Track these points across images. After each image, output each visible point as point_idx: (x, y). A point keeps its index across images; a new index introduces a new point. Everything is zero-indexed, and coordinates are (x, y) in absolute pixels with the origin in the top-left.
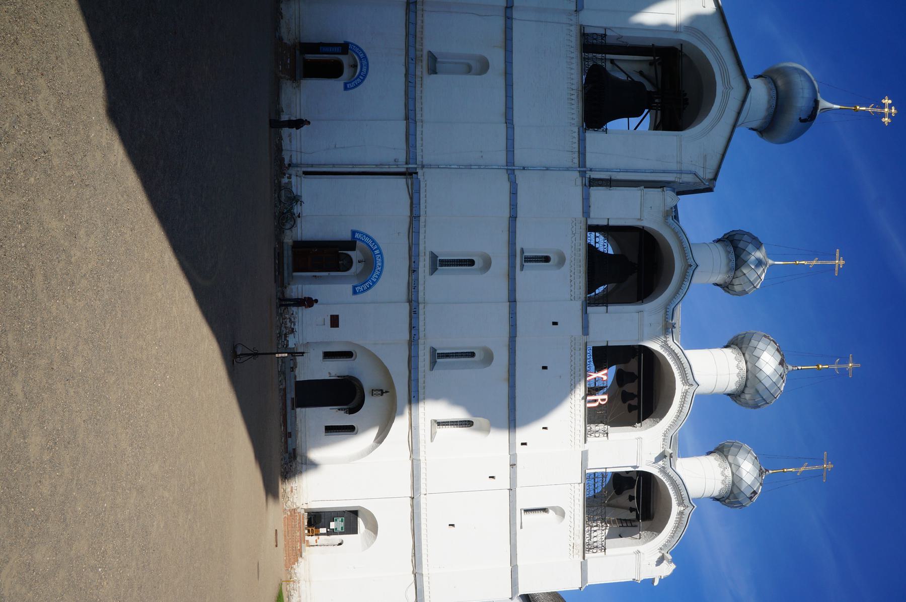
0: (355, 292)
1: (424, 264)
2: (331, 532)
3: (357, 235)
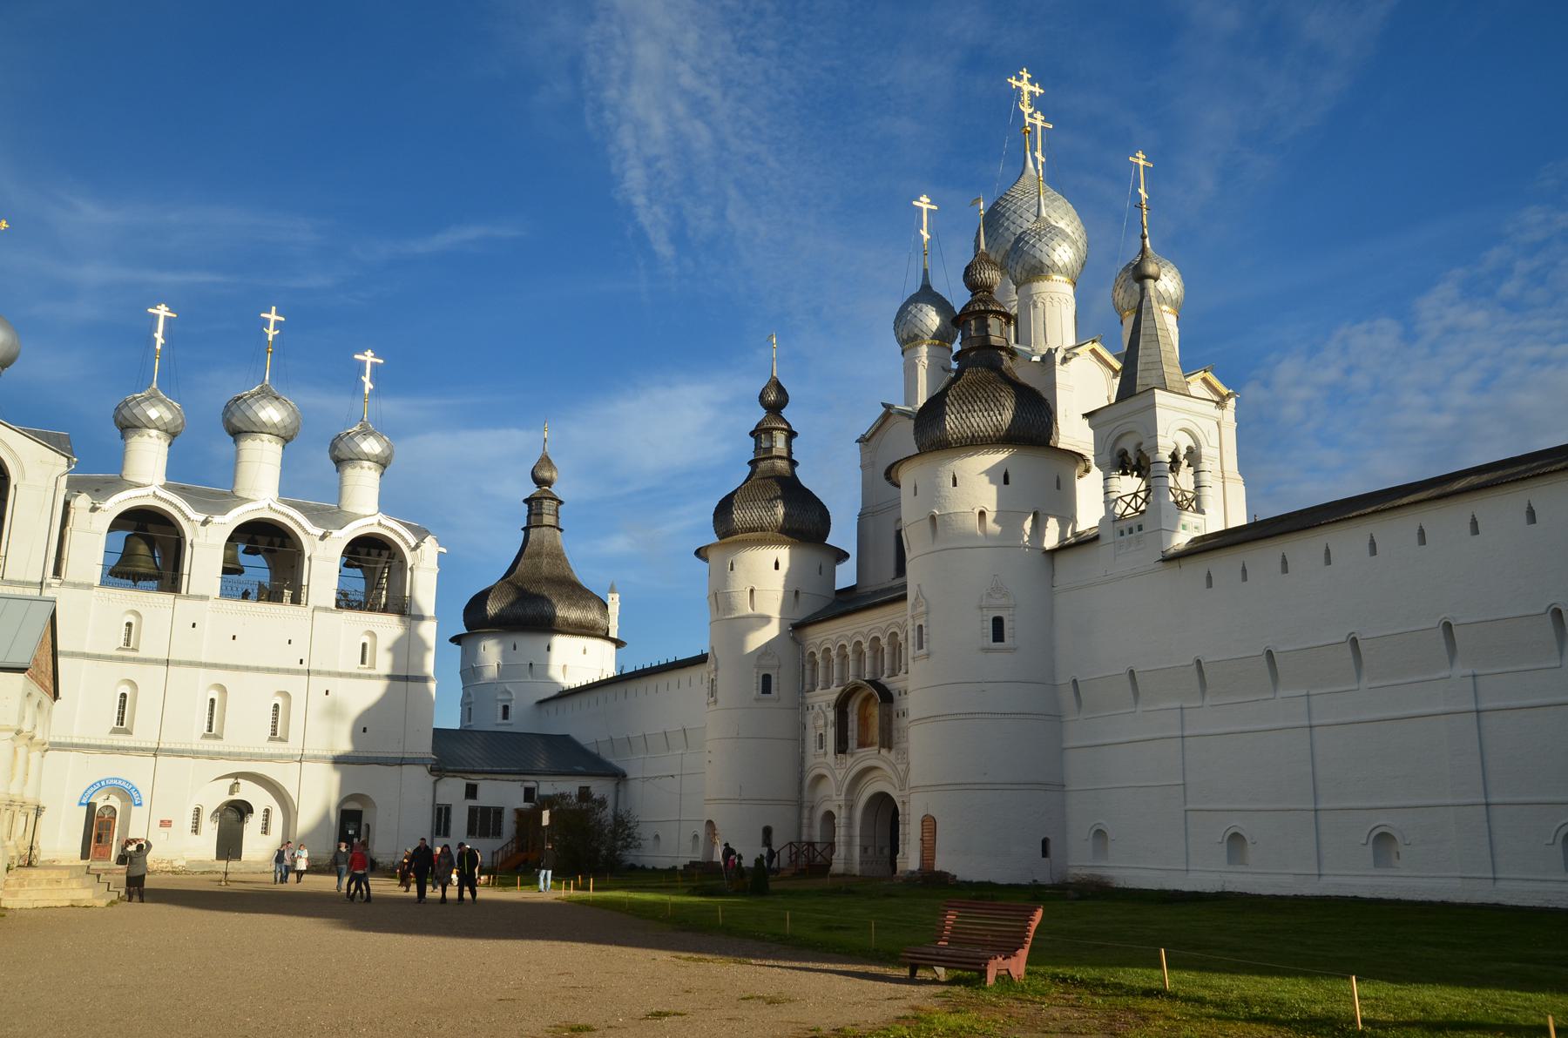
0: (140, 804)
2: (358, 834)
3: (84, 801)
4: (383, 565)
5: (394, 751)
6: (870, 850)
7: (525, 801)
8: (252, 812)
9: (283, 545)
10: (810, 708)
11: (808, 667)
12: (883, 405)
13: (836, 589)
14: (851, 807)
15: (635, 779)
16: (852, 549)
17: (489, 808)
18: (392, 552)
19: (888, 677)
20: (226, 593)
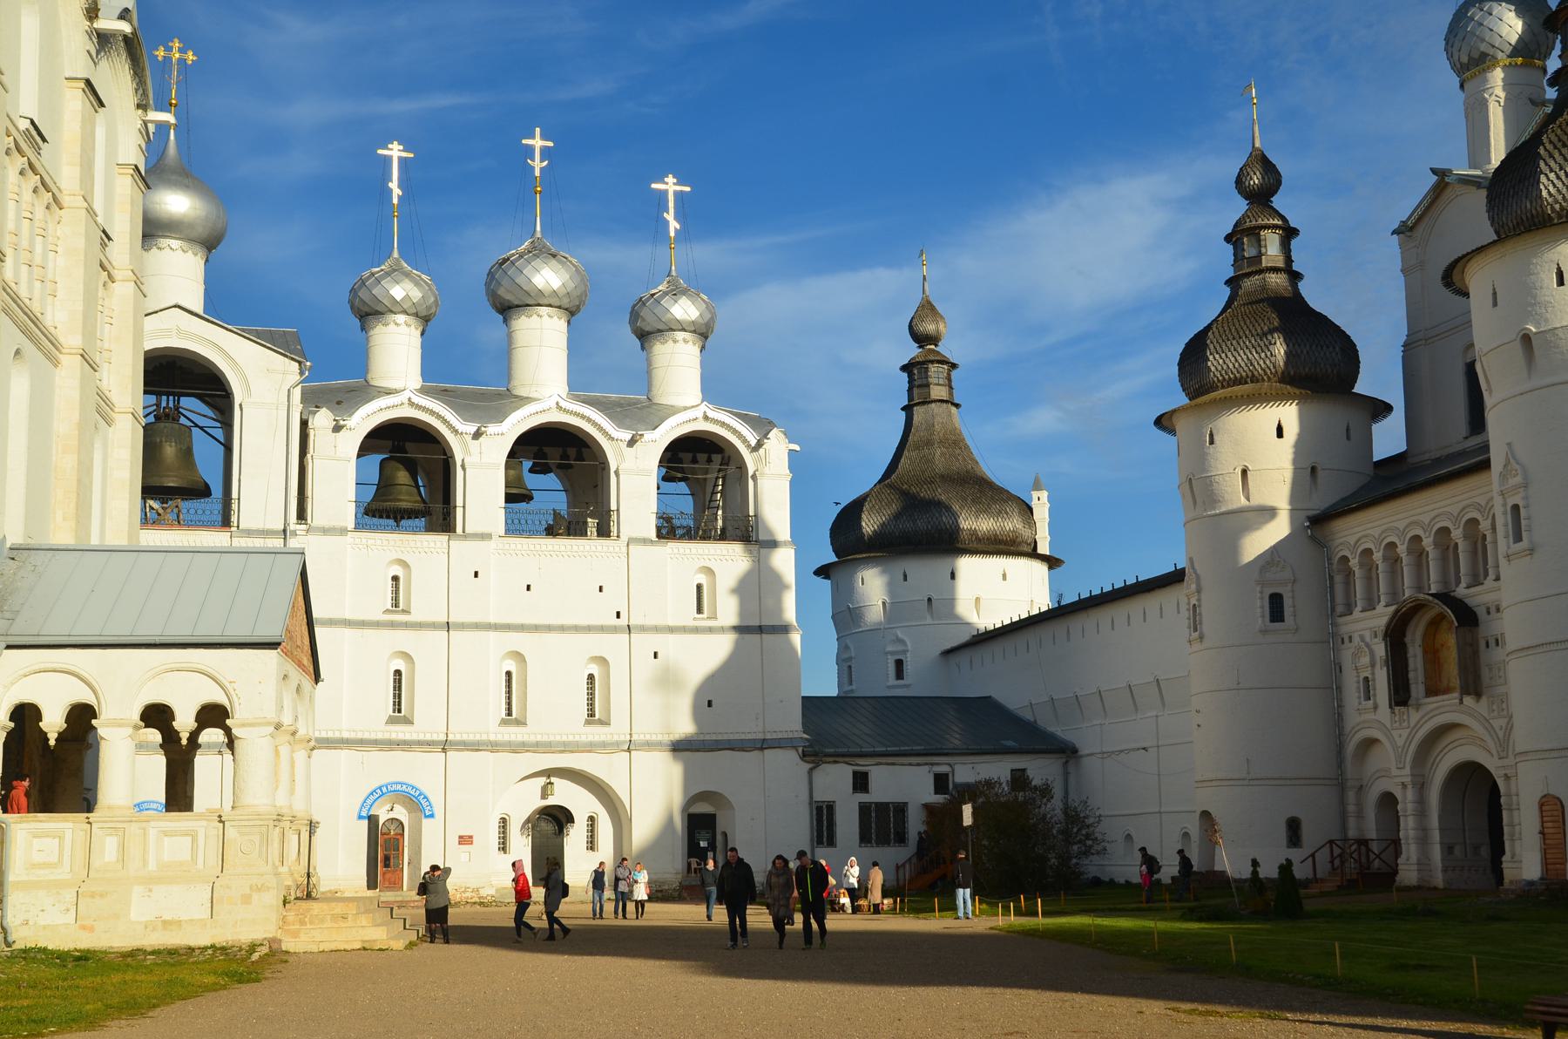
0: (432, 816)
1: (400, 732)
4: (715, 475)
5: (750, 729)
6: (1458, 851)
7: (936, 793)
8: (573, 822)
9: (580, 458)
10: (1346, 640)
11: (1338, 579)
12: (1434, 171)
13: (1375, 460)
14: (1421, 786)
15: (1088, 755)
16: (1396, 398)
17: (887, 804)
18: (726, 455)
19: (1468, 587)
20: (514, 528)
